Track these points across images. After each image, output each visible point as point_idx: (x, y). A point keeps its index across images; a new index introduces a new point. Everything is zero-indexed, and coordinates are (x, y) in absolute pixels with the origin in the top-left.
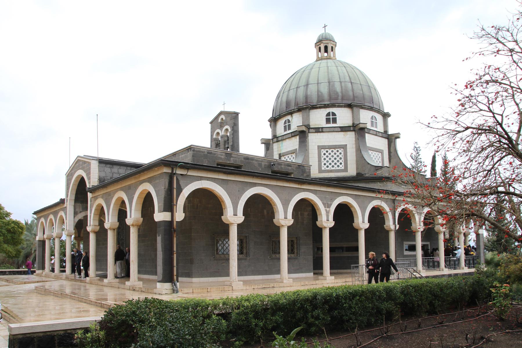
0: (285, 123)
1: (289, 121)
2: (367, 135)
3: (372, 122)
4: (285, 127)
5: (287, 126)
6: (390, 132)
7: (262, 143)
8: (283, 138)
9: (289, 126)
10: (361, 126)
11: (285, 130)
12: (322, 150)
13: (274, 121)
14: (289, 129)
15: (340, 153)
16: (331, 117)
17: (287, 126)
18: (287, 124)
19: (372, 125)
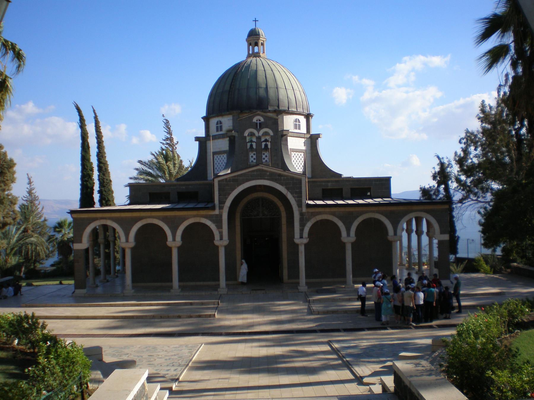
0: (217, 124)
1: (221, 123)
2: (289, 139)
3: (295, 125)
4: (217, 127)
5: (219, 127)
6: (313, 132)
7: (195, 141)
8: (215, 137)
9: (221, 127)
10: (285, 133)
11: (217, 131)
12: (250, 153)
13: (206, 119)
14: (221, 130)
15: (266, 156)
16: (258, 122)
17: (219, 127)
18: (219, 125)
19: (296, 128)
